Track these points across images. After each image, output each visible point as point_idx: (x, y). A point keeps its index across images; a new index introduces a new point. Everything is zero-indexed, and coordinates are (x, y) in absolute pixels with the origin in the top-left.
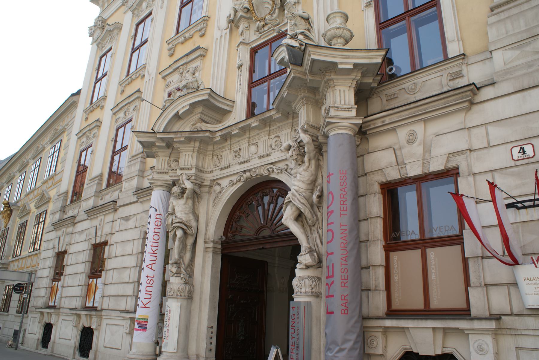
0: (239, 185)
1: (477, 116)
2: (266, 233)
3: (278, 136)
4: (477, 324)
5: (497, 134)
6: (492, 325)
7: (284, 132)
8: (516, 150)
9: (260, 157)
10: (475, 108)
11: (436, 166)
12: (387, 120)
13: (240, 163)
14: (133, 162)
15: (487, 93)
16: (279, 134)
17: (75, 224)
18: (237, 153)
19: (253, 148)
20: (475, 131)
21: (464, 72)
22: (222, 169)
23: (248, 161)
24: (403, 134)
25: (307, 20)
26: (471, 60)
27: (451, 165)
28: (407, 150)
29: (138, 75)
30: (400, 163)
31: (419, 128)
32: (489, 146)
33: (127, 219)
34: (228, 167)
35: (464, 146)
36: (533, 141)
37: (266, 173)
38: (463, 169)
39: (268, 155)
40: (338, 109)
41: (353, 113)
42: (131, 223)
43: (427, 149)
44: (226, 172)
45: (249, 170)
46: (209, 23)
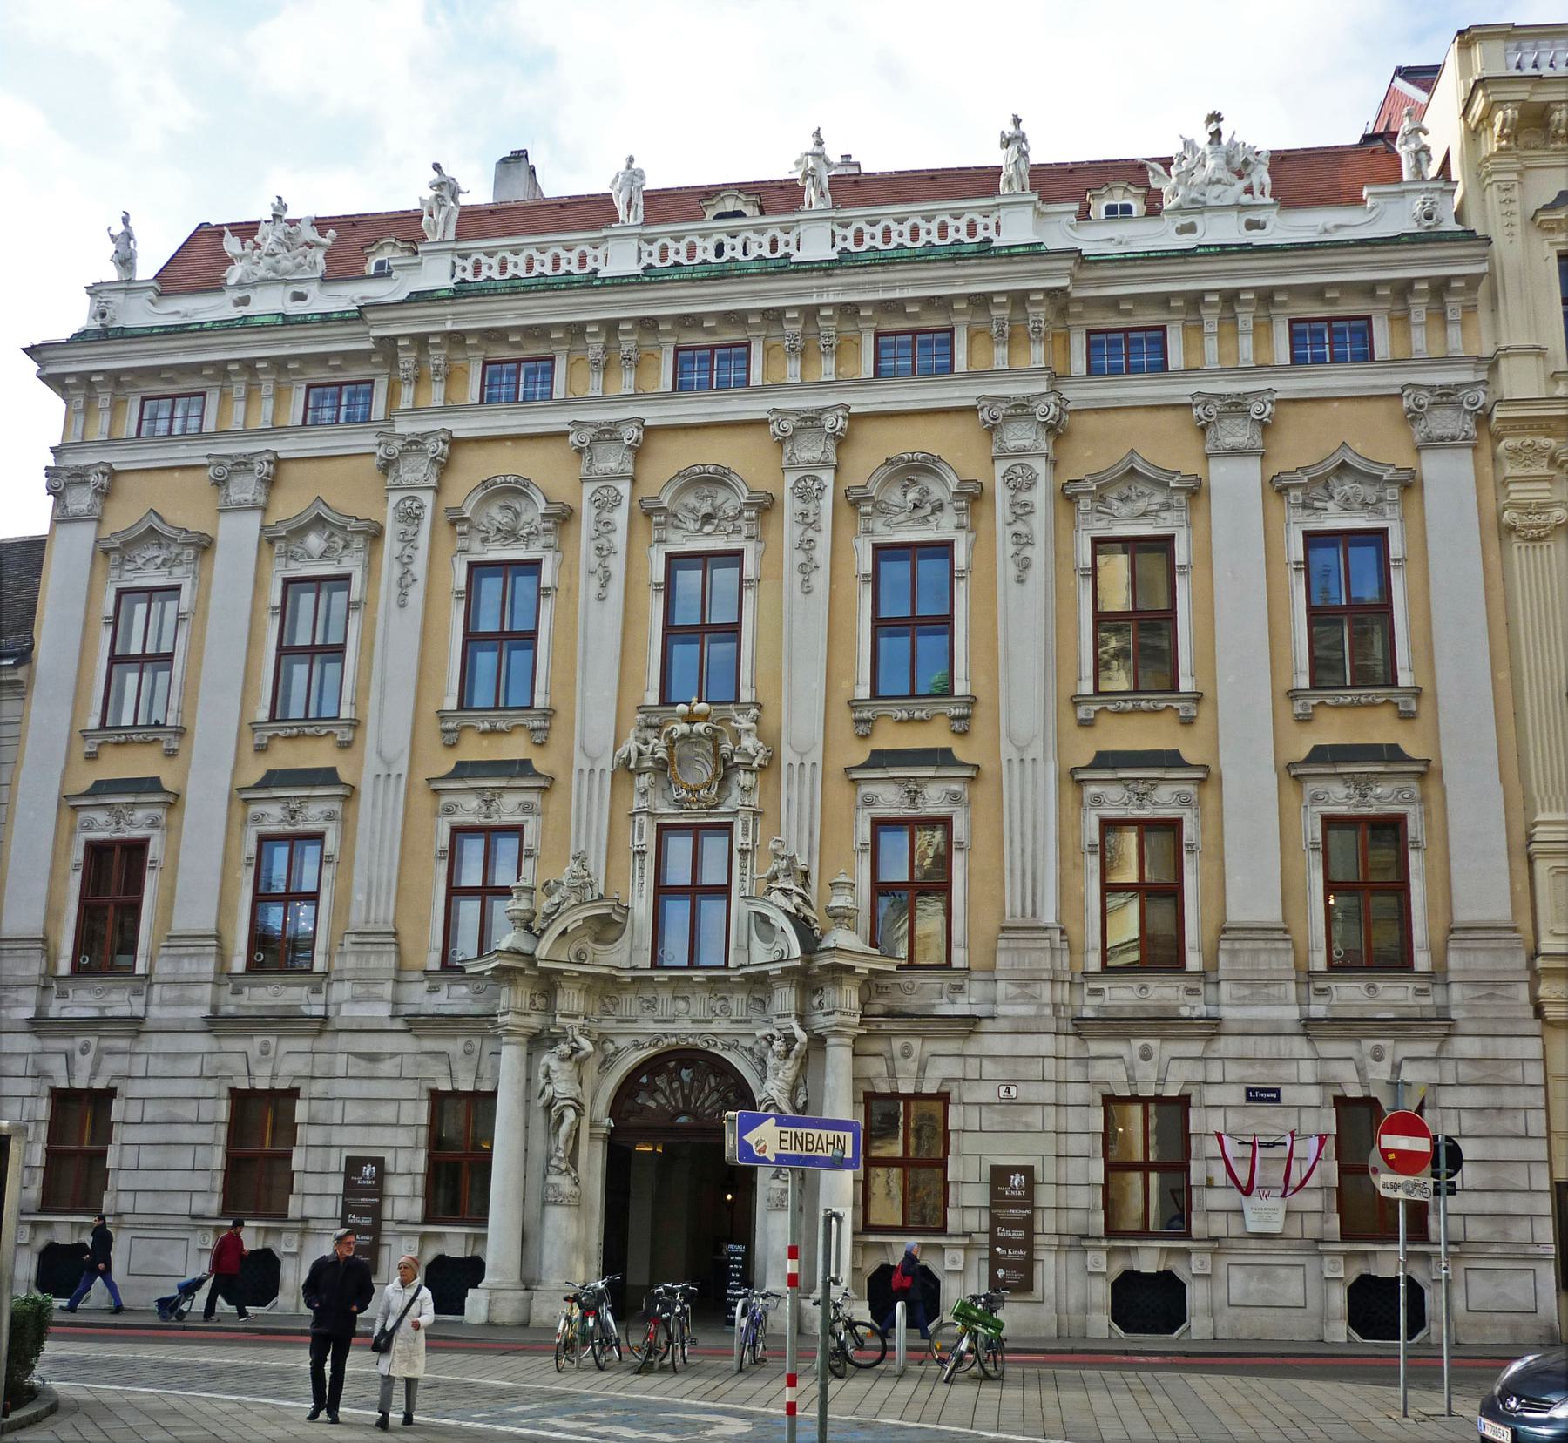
0: (653, 1051)
1: (972, 1048)
2: (683, 1120)
3: (724, 998)
4: (955, 1241)
5: (989, 1069)
6: (966, 1241)
7: (736, 996)
8: (1003, 1089)
9: (694, 1021)
10: (974, 1037)
11: (929, 1088)
12: (884, 1027)
13: (657, 1021)
14: (368, 948)
15: (987, 1025)
16: (727, 995)
17: (139, 1032)
18: (651, 1004)
19: (681, 1005)
20: (970, 1060)
21: (966, 988)
22: (619, 1021)
23: (673, 1021)
24: (897, 1044)
25: (805, 874)
26: (975, 975)
27: (944, 1089)
28: (900, 1063)
29: (323, 732)
30: (892, 1076)
31: (916, 1043)
32: (981, 1079)
33: (373, 1057)
34: (634, 1021)
35: (959, 1075)
36: (1020, 1085)
37: (704, 1046)
38: (954, 1096)
39: (710, 1021)
40: (844, 1013)
41: (857, 1019)
42: (387, 1068)
43: (923, 1068)
44: (627, 1027)
45: (674, 1035)
46: (558, 723)
